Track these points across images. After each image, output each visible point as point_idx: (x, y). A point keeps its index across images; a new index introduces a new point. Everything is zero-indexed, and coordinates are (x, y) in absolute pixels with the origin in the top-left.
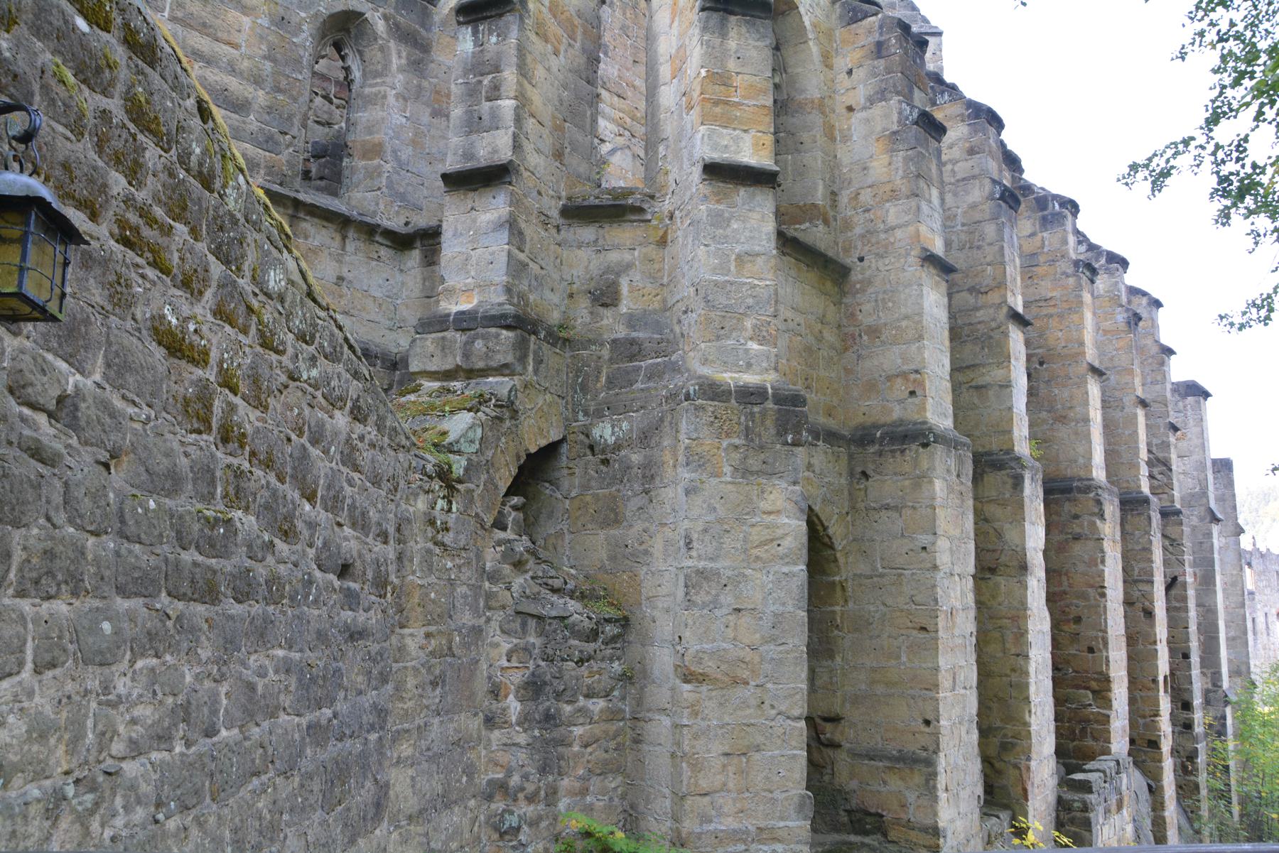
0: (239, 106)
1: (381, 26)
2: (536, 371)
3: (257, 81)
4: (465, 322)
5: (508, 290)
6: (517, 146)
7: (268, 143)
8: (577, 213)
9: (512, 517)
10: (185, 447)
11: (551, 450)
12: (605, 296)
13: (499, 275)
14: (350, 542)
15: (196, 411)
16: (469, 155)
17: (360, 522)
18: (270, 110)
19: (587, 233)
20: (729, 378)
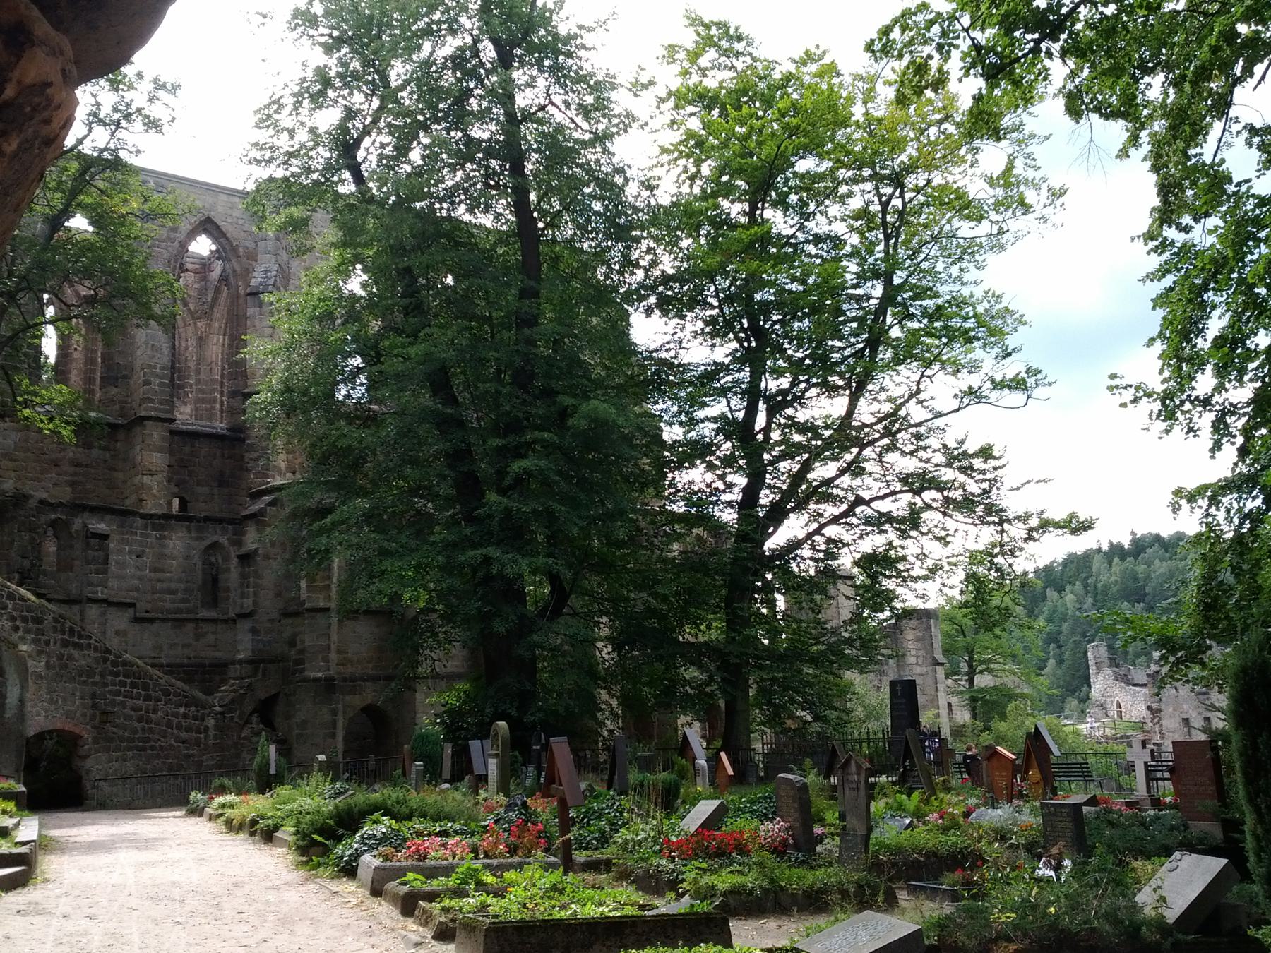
0: (173, 592)
1: (226, 543)
2: (264, 674)
3: (180, 580)
4: (241, 662)
5: (253, 651)
6: (255, 603)
7: (184, 601)
8: (286, 614)
9: (254, 719)
10: (138, 725)
11: (275, 696)
12: (292, 643)
13: (249, 646)
14: (185, 735)
15: (140, 720)
16: (242, 607)
17: (188, 730)
18: (185, 590)
19: (290, 621)
20: (312, 675)
